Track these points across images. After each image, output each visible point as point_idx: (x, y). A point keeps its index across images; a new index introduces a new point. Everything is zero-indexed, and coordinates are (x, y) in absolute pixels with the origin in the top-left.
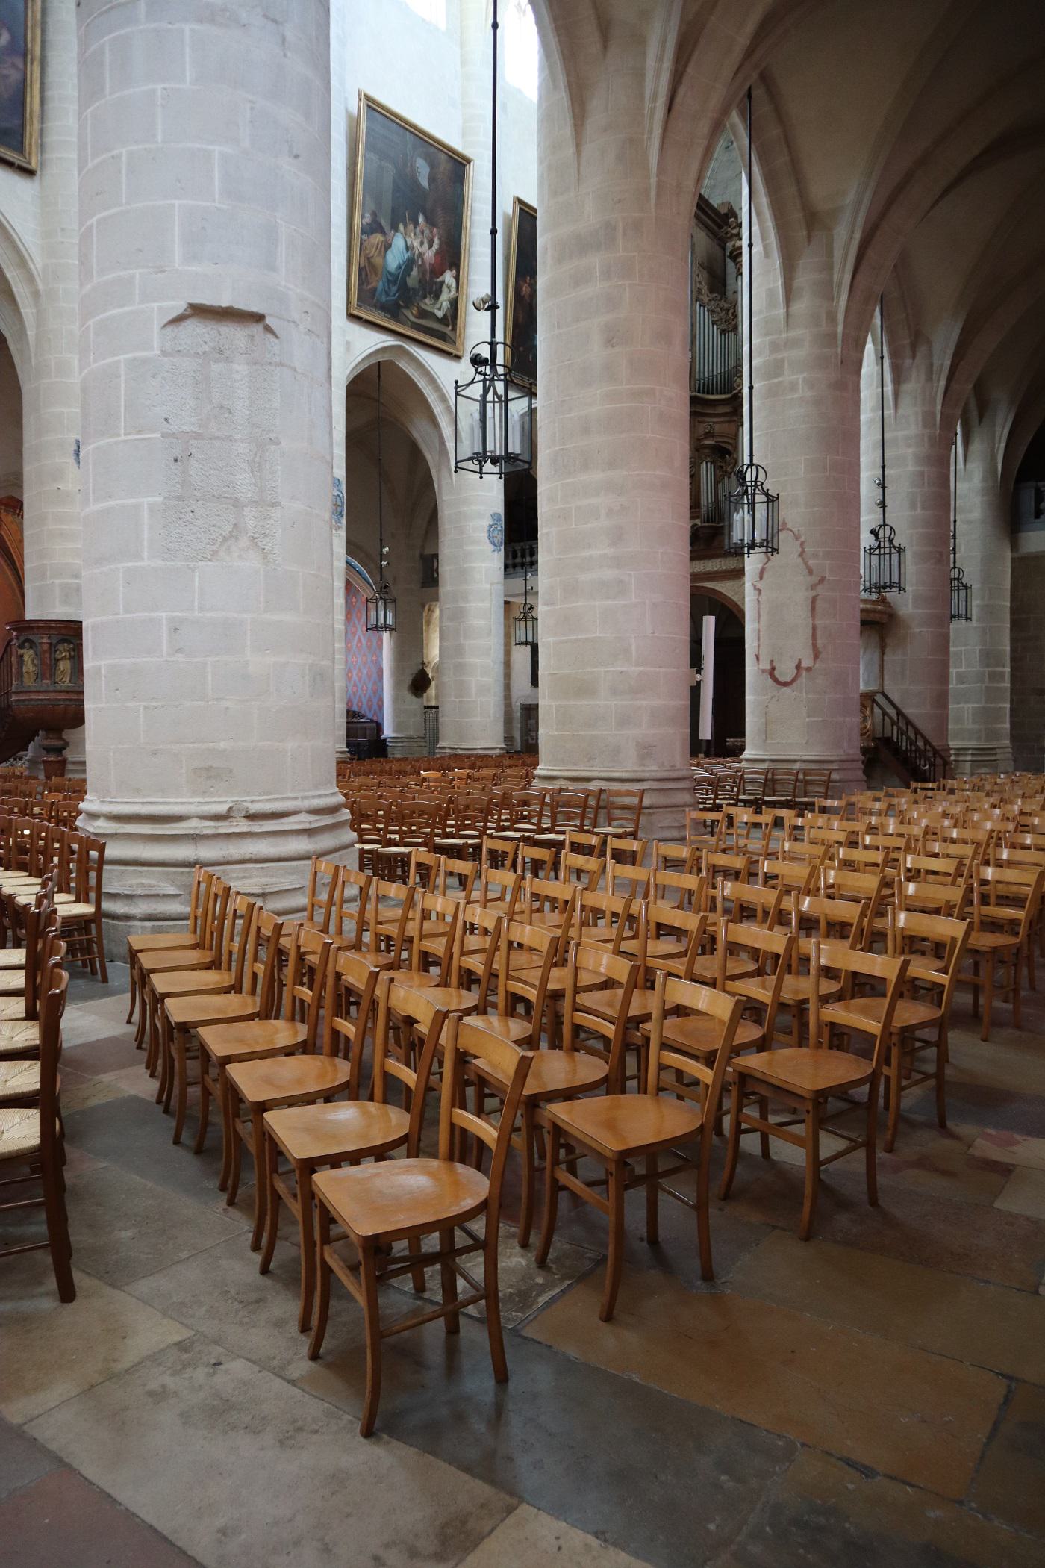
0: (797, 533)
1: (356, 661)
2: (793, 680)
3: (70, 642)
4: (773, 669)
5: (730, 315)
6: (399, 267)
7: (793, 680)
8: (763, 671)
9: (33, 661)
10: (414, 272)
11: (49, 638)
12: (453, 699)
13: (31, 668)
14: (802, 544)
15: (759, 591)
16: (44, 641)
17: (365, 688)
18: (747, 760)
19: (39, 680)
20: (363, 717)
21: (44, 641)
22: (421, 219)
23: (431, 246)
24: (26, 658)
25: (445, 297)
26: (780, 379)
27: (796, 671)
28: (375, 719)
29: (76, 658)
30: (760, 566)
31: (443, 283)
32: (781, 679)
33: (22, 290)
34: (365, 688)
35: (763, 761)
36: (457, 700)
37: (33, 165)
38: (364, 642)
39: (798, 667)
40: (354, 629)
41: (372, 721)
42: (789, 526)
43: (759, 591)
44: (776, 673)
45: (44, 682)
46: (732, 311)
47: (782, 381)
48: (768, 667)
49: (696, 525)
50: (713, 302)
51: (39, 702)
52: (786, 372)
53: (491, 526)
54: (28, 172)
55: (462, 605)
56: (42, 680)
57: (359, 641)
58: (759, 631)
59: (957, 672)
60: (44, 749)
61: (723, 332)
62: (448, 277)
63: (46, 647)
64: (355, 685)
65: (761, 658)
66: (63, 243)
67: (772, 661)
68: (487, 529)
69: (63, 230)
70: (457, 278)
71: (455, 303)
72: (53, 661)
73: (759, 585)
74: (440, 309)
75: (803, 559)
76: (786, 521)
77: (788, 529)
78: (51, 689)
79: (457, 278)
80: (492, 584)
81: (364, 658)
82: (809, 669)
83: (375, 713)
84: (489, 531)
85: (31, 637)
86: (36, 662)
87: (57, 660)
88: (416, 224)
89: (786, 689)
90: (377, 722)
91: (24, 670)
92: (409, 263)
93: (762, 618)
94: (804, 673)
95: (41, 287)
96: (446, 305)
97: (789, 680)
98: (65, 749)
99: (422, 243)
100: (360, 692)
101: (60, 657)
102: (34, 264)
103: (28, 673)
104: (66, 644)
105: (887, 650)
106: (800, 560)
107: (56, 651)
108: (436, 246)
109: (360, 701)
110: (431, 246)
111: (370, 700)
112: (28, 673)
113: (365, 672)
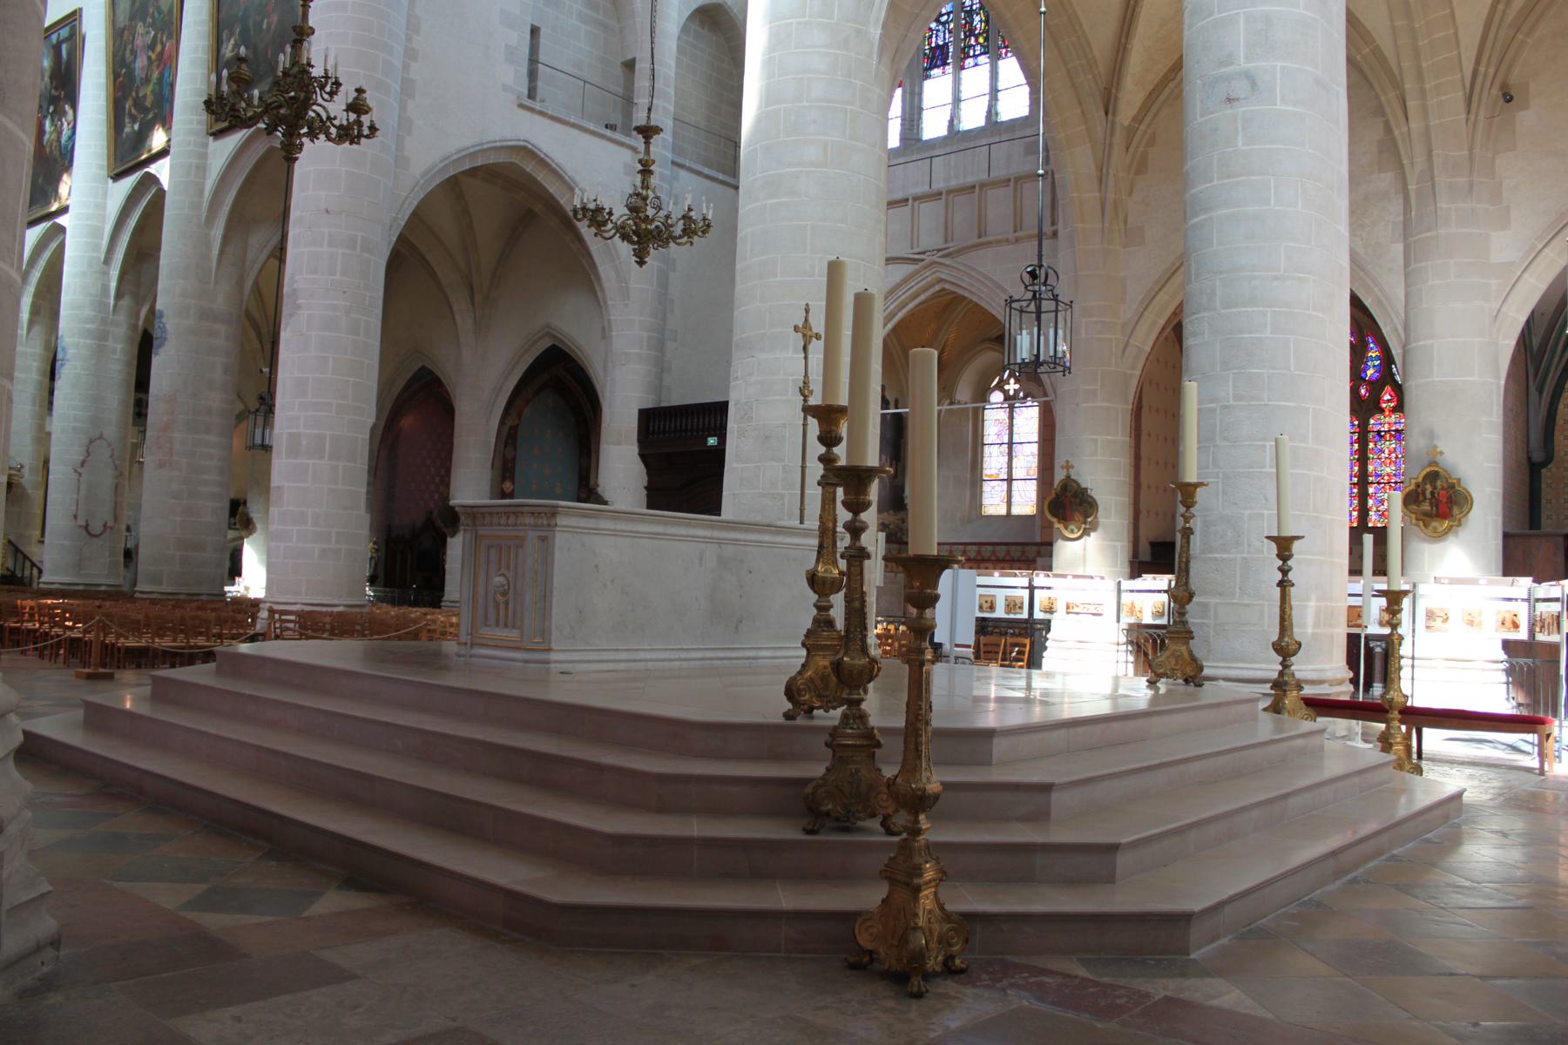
2: (101, 534)
4: (87, 525)
7: (101, 534)
8: (80, 526)
14: (113, 450)
15: (80, 474)
18: (44, 583)
27: (102, 528)
30: (81, 458)
32: (93, 532)
35: (78, 584)
39: (105, 526)
42: (105, 436)
43: (80, 474)
44: (90, 528)
48: (84, 524)
67: (87, 521)
73: (79, 470)
82: (111, 528)
89: (95, 539)
93: (81, 493)
94: (108, 530)
97: (98, 533)
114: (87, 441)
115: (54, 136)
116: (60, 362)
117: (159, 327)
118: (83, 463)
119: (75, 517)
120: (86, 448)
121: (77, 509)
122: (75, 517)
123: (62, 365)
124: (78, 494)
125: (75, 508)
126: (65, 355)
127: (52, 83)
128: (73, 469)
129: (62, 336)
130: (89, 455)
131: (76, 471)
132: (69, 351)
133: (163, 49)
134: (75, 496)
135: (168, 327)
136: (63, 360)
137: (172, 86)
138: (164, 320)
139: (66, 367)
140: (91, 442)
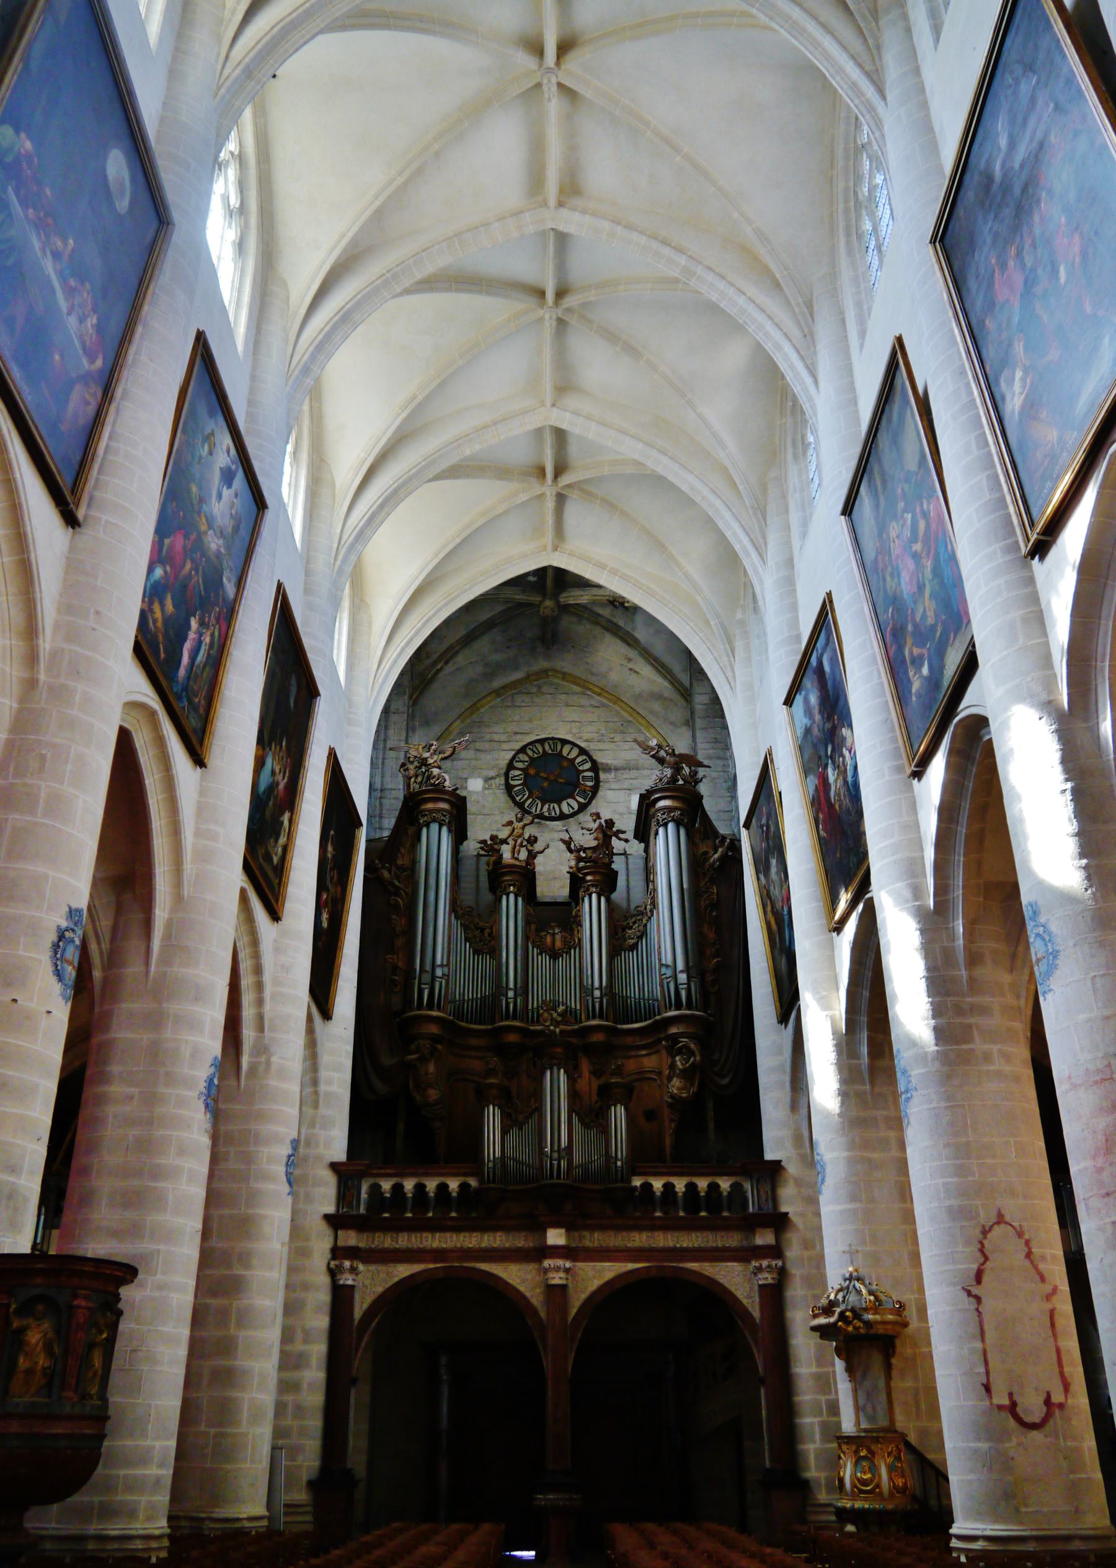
0: (1018, 1229)
4: (1013, 1405)
5: (486, 935)
6: (264, 792)
8: (1000, 1407)
9: (48, 1348)
10: (271, 804)
12: (203, 1428)
14: (1027, 1243)
21: (83, 1303)
22: (284, 744)
23: (284, 778)
25: (282, 840)
26: (971, 1046)
27: (1045, 1409)
30: (975, 1266)
31: (283, 823)
33: (8, 669)
36: (212, 1431)
37: (81, 514)
39: (1048, 1401)
42: (1008, 1218)
43: (978, 1299)
44: (1019, 1410)
46: (487, 931)
47: (972, 1050)
48: (1006, 1402)
49: (469, 1185)
50: (467, 917)
52: (977, 1041)
53: (289, 1157)
54: (70, 519)
55: (238, 1271)
58: (985, 1353)
59: (827, 1400)
61: (477, 952)
62: (286, 818)
65: (994, 1389)
66: (94, 629)
67: (1011, 1395)
68: (285, 1160)
69: (97, 613)
70: (291, 821)
71: (285, 849)
74: (276, 854)
75: (1032, 1262)
76: (1003, 1212)
77: (1007, 1223)
79: (291, 821)
80: (283, 1244)
82: (1061, 1406)
84: (287, 1165)
86: (56, 1350)
87: (91, 1346)
88: (281, 747)
89: (1035, 1434)
92: (273, 786)
93: (988, 1336)
94: (1057, 1412)
95: (42, 677)
96: (280, 850)
97: (1037, 1420)
99: (280, 770)
102: (44, 641)
103: (29, 1372)
105: (894, 1373)
106: (1027, 1263)
108: (286, 780)
110: (284, 778)
114: (977, 1232)
115: (840, 782)
116: (903, 1096)
117: (1038, 935)
118: (979, 1277)
119: (987, 1388)
120: (979, 1246)
121: (988, 1373)
122: (987, 1388)
123: (908, 1100)
124: (983, 1340)
125: (982, 1370)
126: (909, 1082)
127: (823, 717)
128: (963, 1288)
129: (898, 1051)
130: (986, 1259)
131: (969, 1293)
132: (914, 1073)
133: (928, 526)
134: (978, 1345)
135: (1054, 927)
136: (907, 1091)
137: (953, 559)
138: (1042, 919)
139: (914, 1101)
140: (985, 1232)
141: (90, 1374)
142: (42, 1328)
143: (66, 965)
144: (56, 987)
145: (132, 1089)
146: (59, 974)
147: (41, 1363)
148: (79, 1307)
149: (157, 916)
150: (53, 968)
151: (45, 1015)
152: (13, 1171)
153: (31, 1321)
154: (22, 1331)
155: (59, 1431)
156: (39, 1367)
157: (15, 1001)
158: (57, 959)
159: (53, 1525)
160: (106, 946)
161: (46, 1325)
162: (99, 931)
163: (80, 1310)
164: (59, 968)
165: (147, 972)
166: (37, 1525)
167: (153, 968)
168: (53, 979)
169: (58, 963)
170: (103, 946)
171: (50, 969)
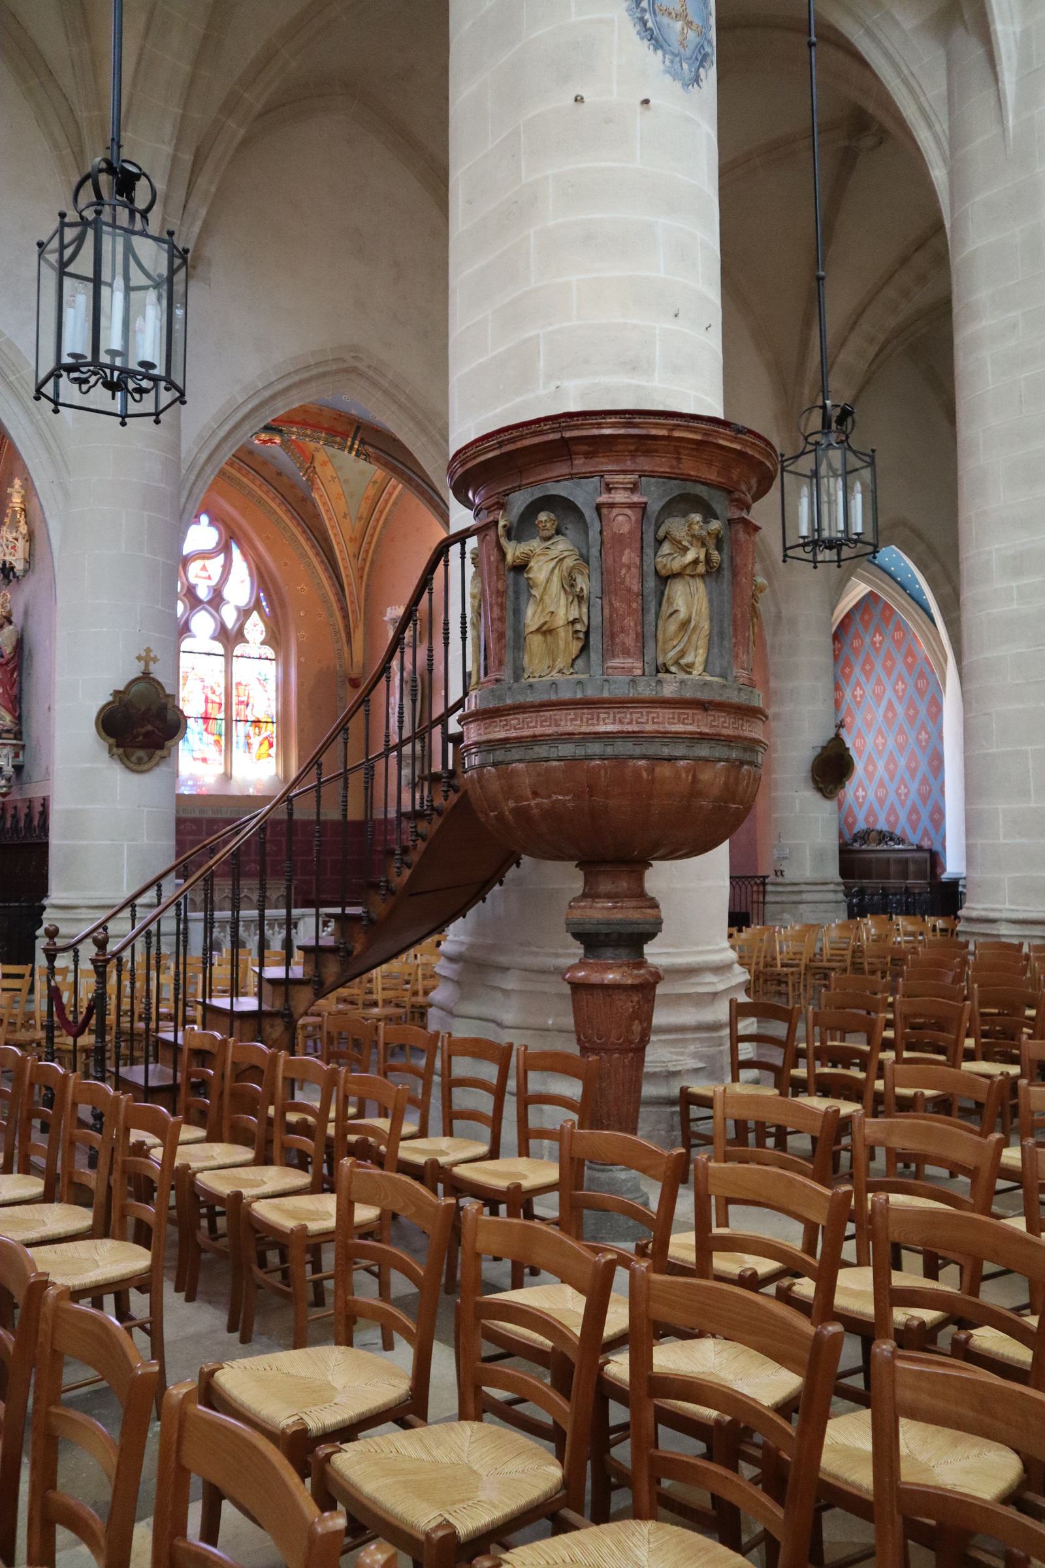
1: (884, 745)
3: (709, 514)
9: (569, 583)
11: (634, 488)
13: (563, 611)
16: (620, 497)
17: (903, 790)
19: (595, 656)
20: (901, 841)
21: (620, 497)
24: (540, 571)
28: (926, 844)
29: (727, 573)
34: (903, 790)
38: (900, 709)
40: (878, 689)
41: (920, 849)
45: (617, 662)
51: (595, 748)
56: (607, 654)
57: (890, 707)
60: (576, 936)
63: (623, 522)
64: (881, 784)
72: (651, 583)
78: (645, 690)
81: (900, 739)
83: (926, 833)
85: (561, 489)
86: (582, 583)
87: (665, 579)
90: (930, 851)
91: (532, 617)
98: (651, 936)
100: (892, 797)
101: (676, 565)
103: (546, 631)
104: (697, 517)
107: (659, 542)
109: (892, 810)
111: (914, 810)
112: (546, 631)
113: (902, 762)
141: (672, 627)
142: (553, 553)
143: (665, 20)
144: (655, 60)
145: (1014, 314)
146: (655, 39)
147: (562, 612)
148: (612, 505)
149: (1000, 35)
150: (638, 28)
151: (639, 108)
152: (634, 369)
153: (535, 544)
154: (521, 568)
155: (610, 728)
156: (560, 619)
157: (579, 99)
158: (644, 10)
159: (1007, 906)
160: (942, 127)
161: (561, 546)
162: (928, 109)
163: (615, 511)
164: (650, 24)
165: (1004, 130)
166: (988, 906)
167: (1011, 121)
168: (643, 48)
169: (647, 16)
170: (938, 128)
171: (631, 30)
